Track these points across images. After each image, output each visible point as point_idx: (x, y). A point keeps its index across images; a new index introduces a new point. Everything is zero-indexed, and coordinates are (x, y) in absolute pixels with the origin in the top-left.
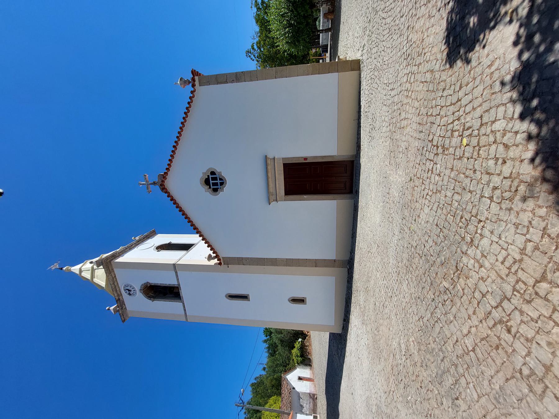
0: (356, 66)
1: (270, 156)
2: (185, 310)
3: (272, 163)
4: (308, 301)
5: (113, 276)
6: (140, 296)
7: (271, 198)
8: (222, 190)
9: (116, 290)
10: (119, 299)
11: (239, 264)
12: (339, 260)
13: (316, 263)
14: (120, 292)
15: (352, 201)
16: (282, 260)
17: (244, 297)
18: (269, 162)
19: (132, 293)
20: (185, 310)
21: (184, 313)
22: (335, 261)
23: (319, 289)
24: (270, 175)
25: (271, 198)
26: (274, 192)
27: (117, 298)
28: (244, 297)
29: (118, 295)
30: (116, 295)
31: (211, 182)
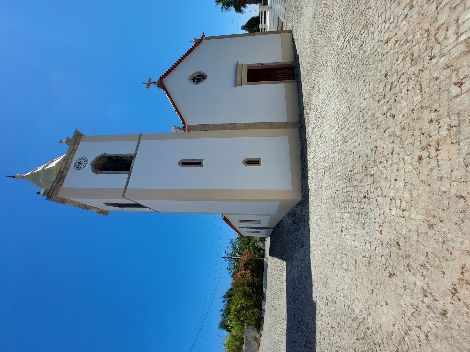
0: (290, 31)
1: (240, 63)
2: (127, 183)
3: (241, 67)
4: (263, 162)
5: (75, 148)
6: (88, 168)
7: (237, 83)
8: (203, 81)
9: (67, 162)
10: (63, 172)
11: (201, 130)
12: (290, 122)
13: (270, 126)
14: (69, 166)
15: (296, 83)
16: (240, 124)
17: (198, 163)
18: (239, 65)
19: (81, 166)
20: (127, 183)
21: (124, 187)
22: (287, 123)
23: (274, 149)
24: (238, 71)
25: (237, 83)
26: (240, 80)
27: (62, 169)
28: (198, 163)
29: (66, 167)
30: (64, 166)
31: (196, 80)
